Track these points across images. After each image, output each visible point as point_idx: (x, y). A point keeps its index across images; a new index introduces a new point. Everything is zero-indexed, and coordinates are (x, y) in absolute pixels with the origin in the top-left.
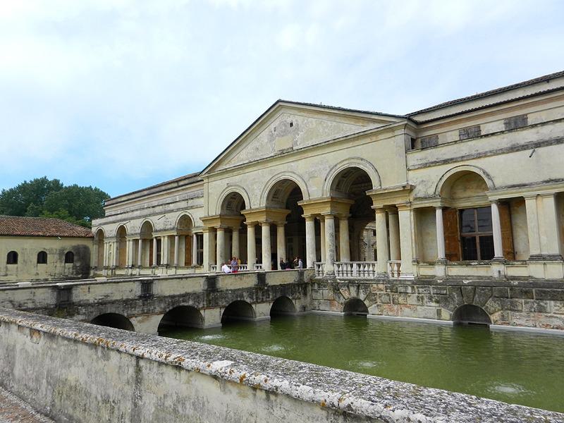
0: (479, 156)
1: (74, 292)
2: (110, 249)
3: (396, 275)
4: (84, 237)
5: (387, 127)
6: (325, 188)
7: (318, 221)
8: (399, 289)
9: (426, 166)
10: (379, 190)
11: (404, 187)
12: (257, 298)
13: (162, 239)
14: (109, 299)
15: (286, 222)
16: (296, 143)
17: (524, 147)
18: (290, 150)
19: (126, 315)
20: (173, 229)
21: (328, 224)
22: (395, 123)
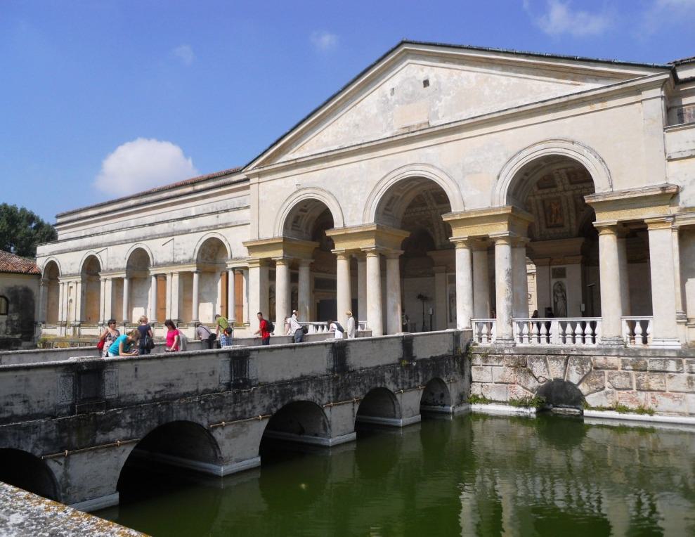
1: (107, 376)
2: (70, 297)
3: (639, 340)
4: (26, 273)
5: (629, 85)
6: (497, 192)
7: (356, 260)
8: (650, 366)
10: (605, 195)
11: (663, 188)
12: (403, 383)
13: (169, 278)
14: (173, 391)
15: (402, 252)
16: (436, 115)
18: (423, 127)
19: (205, 423)
20: (190, 261)
21: (372, 264)
22: (644, 77)
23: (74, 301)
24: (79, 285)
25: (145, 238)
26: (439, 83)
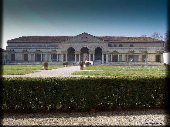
0: (118, 49)
9: (111, 49)
17: (122, 49)
20: (50, 53)
23: (20, 57)
25: (40, 48)
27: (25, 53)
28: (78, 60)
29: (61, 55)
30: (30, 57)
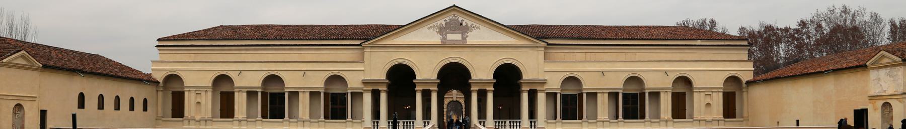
24: (210, 94)
26: (467, 25)
27: (226, 88)
28: (427, 115)
29: (361, 94)
30: (240, 101)
